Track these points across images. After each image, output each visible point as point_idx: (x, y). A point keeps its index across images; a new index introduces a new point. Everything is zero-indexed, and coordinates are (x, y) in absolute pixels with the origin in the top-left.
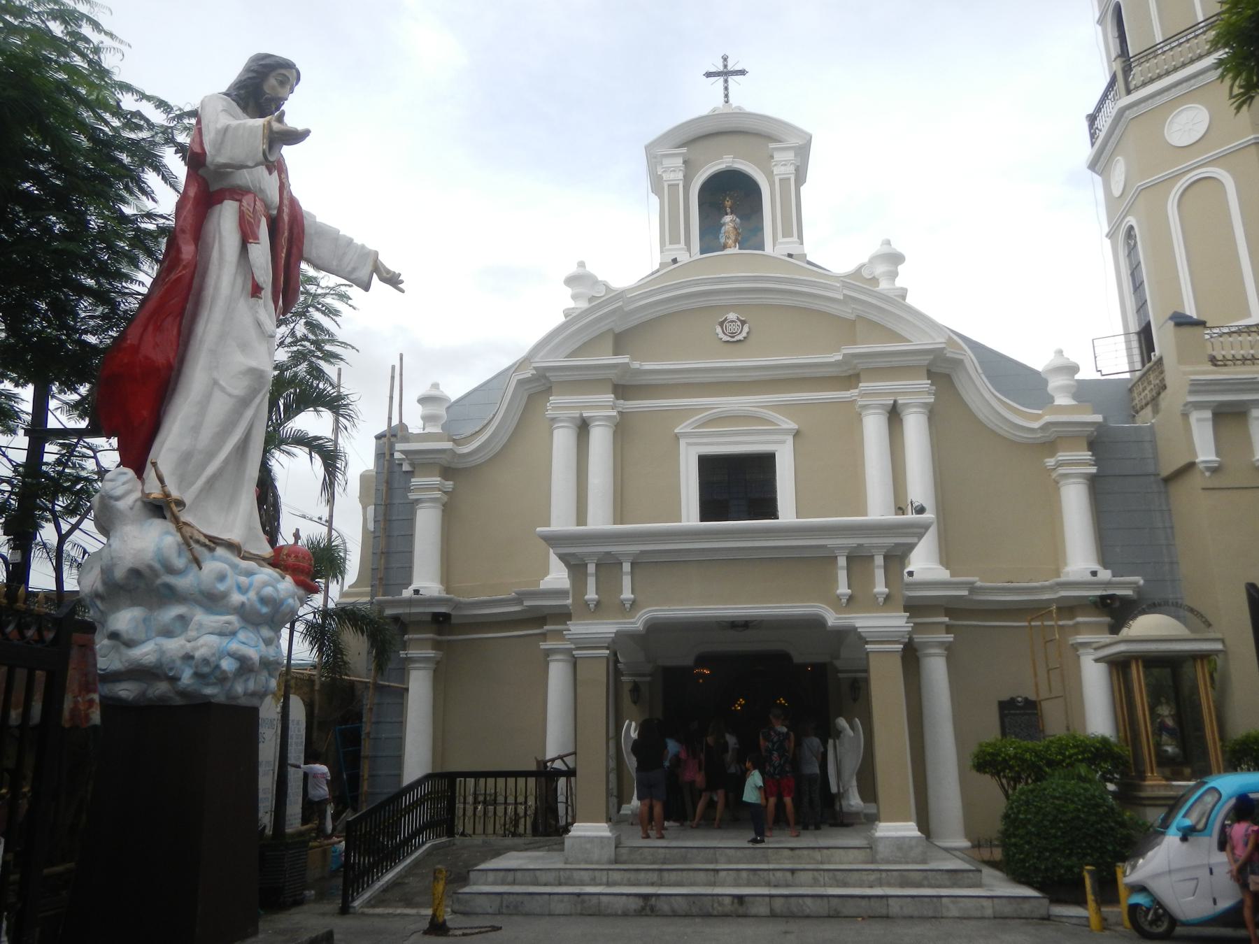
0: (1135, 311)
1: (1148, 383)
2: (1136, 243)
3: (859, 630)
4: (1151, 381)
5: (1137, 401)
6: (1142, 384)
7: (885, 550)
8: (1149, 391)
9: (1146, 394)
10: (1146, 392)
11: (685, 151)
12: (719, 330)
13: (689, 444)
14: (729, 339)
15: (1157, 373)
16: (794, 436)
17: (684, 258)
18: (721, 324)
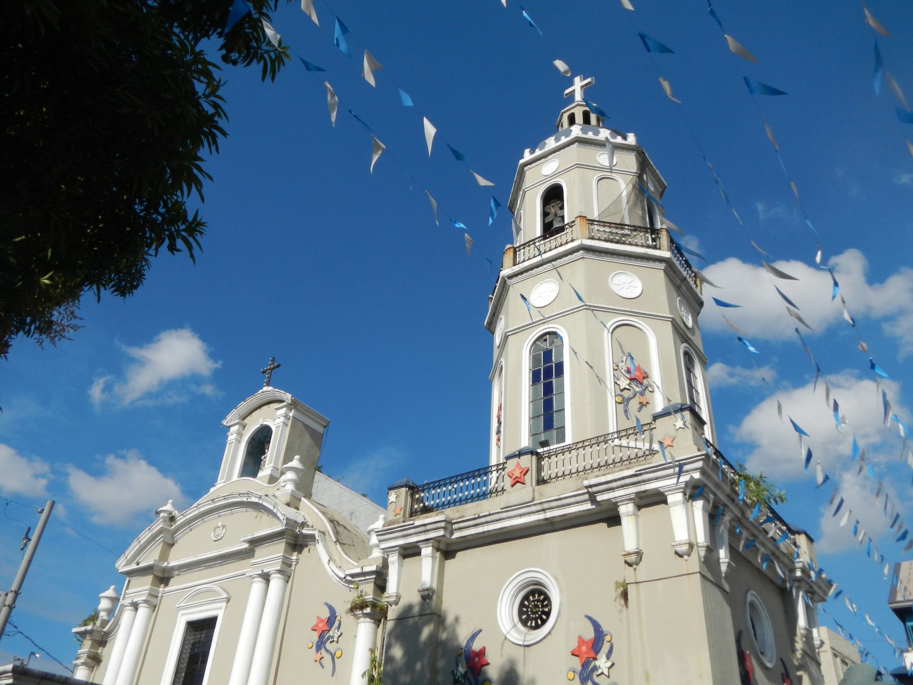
12: (213, 534)
13: (183, 614)
16: (227, 603)
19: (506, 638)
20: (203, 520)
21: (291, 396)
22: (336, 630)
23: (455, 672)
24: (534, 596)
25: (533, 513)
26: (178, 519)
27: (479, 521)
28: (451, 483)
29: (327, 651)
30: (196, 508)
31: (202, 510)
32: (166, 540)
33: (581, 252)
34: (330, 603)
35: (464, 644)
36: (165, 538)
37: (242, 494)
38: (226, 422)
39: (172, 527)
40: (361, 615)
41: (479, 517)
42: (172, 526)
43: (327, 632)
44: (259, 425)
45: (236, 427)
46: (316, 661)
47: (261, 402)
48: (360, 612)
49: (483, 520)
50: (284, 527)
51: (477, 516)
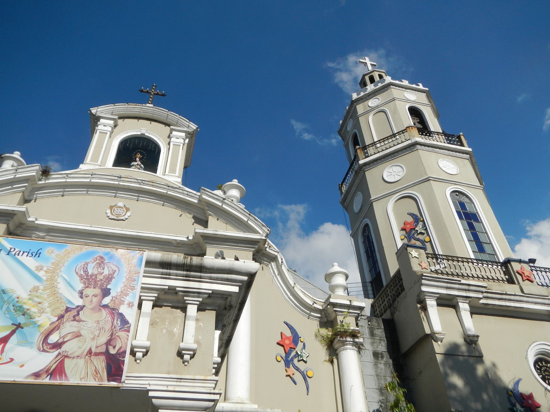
0: (368, 271)
1: (386, 297)
2: (369, 231)
3: (151, 394)
4: (388, 295)
5: (378, 312)
6: (382, 299)
7: (201, 299)
8: (387, 302)
9: (385, 305)
10: (386, 302)
11: (117, 118)
12: (108, 211)
14: (115, 217)
15: (393, 287)
17: (97, 167)
18: (111, 208)
19: (546, 389)
20: (87, 191)
21: (197, 127)
22: (304, 351)
23: (515, 408)
24: (542, 363)
25: (545, 304)
26: (53, 176)
27: (504, 297)
28: (453, 260)
29: (297, 369)
30: (90, 176)
31: (93, 180)
32: (25, 193)
33: (468, 155)
34: (289, 323)
35: (511, 386)
36: (26, 189)
37: (172, 187)
38: (95, 110)
39: (40, 182)
40: (352, 343)
41: (506, 294)
42: (40, 180)
43: (293, 350)
44: (139, 133)
45: (112, 122)
46: (289, 376)
47: (142, 114)
48: (352, 340)
49: (507, 297)
50: (264, 238)
51: (504, 293)
